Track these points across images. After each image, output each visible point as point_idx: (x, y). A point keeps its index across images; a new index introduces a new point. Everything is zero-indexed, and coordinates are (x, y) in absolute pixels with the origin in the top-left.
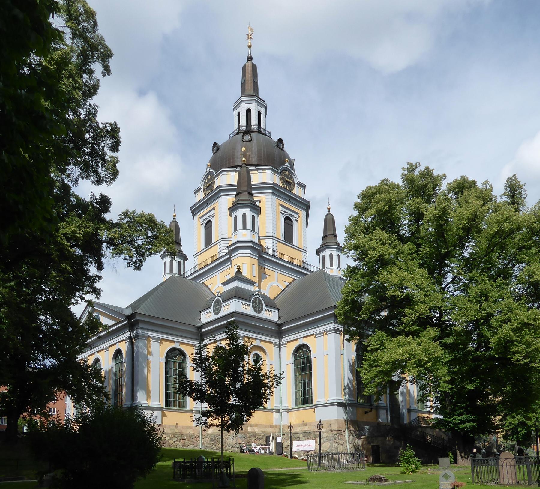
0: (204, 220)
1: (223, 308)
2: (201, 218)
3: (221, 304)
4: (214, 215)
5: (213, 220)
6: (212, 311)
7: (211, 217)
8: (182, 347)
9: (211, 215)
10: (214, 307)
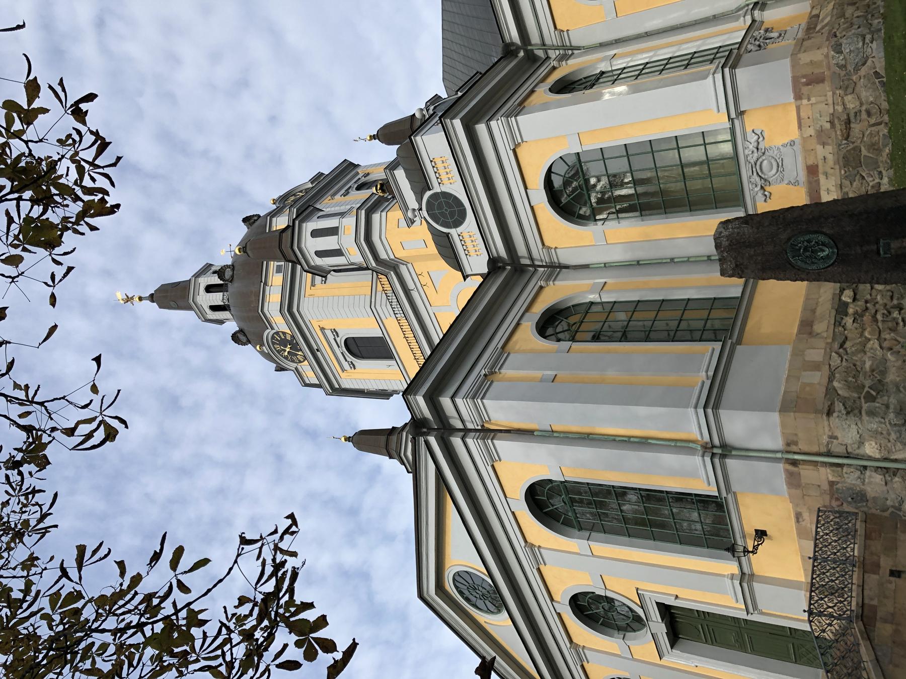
0: (346, 360)
1: (446, 188)
2: (343, 370)
4: (334, 329)
6: (460, 229)
7: (338, 339)
8: (540, 308)
9: (335, 339)
10: (450, 228)
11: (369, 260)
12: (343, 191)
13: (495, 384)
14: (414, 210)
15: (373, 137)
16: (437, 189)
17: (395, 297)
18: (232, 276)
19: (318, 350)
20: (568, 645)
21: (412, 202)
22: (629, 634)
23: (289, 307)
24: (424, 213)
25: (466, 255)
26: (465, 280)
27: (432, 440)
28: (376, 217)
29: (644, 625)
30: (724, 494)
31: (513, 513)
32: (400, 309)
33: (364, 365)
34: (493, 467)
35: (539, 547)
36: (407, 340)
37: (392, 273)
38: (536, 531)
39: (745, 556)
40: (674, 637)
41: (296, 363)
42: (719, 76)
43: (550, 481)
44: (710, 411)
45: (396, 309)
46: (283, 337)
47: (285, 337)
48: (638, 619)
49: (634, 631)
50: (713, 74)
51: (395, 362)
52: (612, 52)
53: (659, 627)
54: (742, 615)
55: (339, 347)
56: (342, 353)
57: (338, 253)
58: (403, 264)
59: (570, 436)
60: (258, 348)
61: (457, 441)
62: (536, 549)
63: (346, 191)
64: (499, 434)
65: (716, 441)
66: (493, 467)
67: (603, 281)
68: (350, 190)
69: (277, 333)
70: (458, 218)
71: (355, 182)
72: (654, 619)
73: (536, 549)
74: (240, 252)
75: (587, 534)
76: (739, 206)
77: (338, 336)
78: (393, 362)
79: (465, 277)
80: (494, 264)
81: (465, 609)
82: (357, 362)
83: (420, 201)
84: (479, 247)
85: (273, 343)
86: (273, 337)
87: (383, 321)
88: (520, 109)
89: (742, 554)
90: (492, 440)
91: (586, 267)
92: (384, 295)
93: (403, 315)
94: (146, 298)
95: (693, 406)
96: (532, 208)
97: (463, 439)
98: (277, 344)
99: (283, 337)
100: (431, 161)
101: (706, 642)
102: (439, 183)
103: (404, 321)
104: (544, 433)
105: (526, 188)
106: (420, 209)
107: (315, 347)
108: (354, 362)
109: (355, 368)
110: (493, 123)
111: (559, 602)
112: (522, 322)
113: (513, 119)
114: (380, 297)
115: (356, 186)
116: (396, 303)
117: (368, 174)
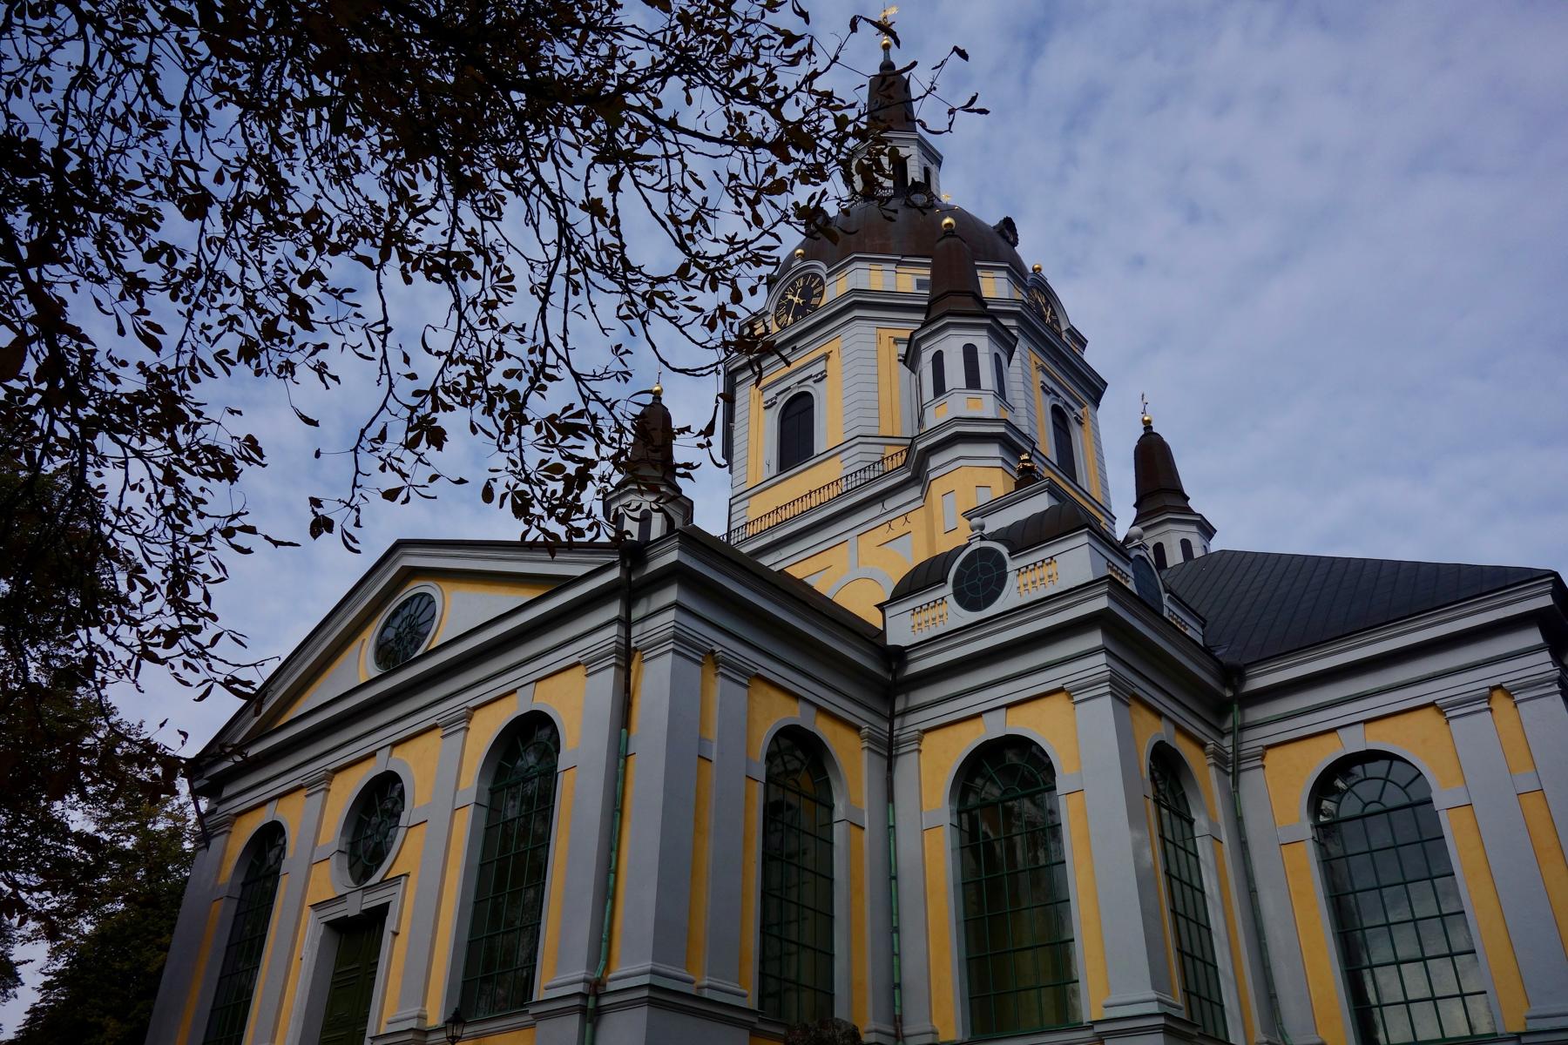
0: (778, 394)
3: (1003, 564)
4: (826, 376)
5: (819, 392)
6: (951, 600)
7: (810, 382)
8: (824, 729)
9: (811, 377)
10: (954, 585)
11: (927, 439)
12: (1050, 384)
13: (697, 669)
14: (982, 527)
15: (1148, 425)
16: (1011, 565)
17: (876, 475)
18: (914, 206)
19: (794, 348)
20: (331, 767)
21: (995, 523)
22: (345, 859)
23: (861, 303)
24: (976, 545)
25: (914, 609)
26: (878, 606)
27: (615, 574)
28: (994, 450)
29: (358, 882)
30: (532, 1010)
31: (514, 692)
32: (854, 485)
33: (771, 420)
34: (577, 664)
35: (467, 729)
36: (806, 496)
37: (909, 474)
38: (489, 726)
39: (447, 1038)
40: (339, 928)
41: (776, 313)
42: (1154, 1008)
43: (558, 751)
44: (645, 993)
45: (854, 479)
46: (815, 292)
47: (816, 296)
48: (367, 874)
49: (351, 868)
50: (1158, 1000)
51: (775, 474)
52: (1224, 838)
53: (354, 906)
54: (371, 1030)
55: (799, 383)
56: (789, 388)
57: (939, 388)
58: (922, 493)
59: (619, 784)
60: (799, 251)
61: (614, 610)
62: (464, 725)
63: (1052, 389)
64: (623, 675)
65: (605, 1001)
66: (577, 664)
67: (866, 826)
68: (1052, 396)
69: (822, 283)
70: (968, 599)
71: (1066, 403)
72: (366, 899)
73: (464, 725)
74: (947, 225)
75: (485, 801)
76: (973, 1033)
77: (815, 382)
78: (774, 471)
79: (881, 607)
80: (899, 655)
81: (382, 610)
82: (776, 410)
83: (994, 537)
84: (925, 630)
85: (806, 276)
86: (815, 276)
87: (838, 457)
88: (1123, 695)
89: (450, 1034)
90: (615, 664)
91: (890, 797)
92: (878, 458)
93: (844, 490)
94: (887, 56)
95: (656, 968)
96: (978, 715)
97: (617, 620)
98: (804, 283)
99: (815, 292)
100: (1051, 558)
101: (335, 974)
102: (1019, 570)
103: (835, 491)
104: (623, 741)
105: (1008, 706)
106: (983, 538)
107: (799, 345)
108: (775, 406)
109: (765, 408)
110: (1102, 658)
111: (390, 754)
112: (801, 703)
113: (1107, 689)
114: (873, 452)
115: (1060, 405)
116: (867, 477)
117: (1080, 424)
